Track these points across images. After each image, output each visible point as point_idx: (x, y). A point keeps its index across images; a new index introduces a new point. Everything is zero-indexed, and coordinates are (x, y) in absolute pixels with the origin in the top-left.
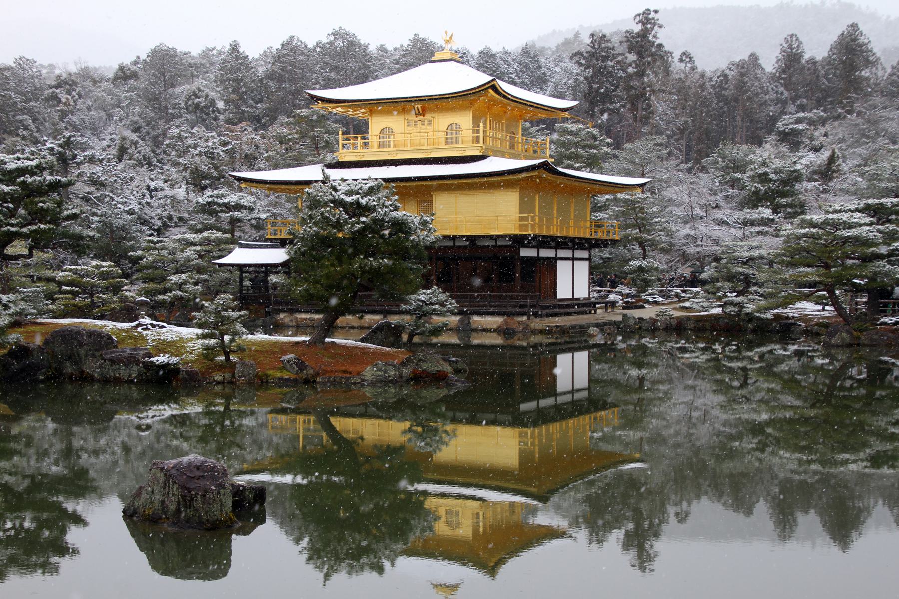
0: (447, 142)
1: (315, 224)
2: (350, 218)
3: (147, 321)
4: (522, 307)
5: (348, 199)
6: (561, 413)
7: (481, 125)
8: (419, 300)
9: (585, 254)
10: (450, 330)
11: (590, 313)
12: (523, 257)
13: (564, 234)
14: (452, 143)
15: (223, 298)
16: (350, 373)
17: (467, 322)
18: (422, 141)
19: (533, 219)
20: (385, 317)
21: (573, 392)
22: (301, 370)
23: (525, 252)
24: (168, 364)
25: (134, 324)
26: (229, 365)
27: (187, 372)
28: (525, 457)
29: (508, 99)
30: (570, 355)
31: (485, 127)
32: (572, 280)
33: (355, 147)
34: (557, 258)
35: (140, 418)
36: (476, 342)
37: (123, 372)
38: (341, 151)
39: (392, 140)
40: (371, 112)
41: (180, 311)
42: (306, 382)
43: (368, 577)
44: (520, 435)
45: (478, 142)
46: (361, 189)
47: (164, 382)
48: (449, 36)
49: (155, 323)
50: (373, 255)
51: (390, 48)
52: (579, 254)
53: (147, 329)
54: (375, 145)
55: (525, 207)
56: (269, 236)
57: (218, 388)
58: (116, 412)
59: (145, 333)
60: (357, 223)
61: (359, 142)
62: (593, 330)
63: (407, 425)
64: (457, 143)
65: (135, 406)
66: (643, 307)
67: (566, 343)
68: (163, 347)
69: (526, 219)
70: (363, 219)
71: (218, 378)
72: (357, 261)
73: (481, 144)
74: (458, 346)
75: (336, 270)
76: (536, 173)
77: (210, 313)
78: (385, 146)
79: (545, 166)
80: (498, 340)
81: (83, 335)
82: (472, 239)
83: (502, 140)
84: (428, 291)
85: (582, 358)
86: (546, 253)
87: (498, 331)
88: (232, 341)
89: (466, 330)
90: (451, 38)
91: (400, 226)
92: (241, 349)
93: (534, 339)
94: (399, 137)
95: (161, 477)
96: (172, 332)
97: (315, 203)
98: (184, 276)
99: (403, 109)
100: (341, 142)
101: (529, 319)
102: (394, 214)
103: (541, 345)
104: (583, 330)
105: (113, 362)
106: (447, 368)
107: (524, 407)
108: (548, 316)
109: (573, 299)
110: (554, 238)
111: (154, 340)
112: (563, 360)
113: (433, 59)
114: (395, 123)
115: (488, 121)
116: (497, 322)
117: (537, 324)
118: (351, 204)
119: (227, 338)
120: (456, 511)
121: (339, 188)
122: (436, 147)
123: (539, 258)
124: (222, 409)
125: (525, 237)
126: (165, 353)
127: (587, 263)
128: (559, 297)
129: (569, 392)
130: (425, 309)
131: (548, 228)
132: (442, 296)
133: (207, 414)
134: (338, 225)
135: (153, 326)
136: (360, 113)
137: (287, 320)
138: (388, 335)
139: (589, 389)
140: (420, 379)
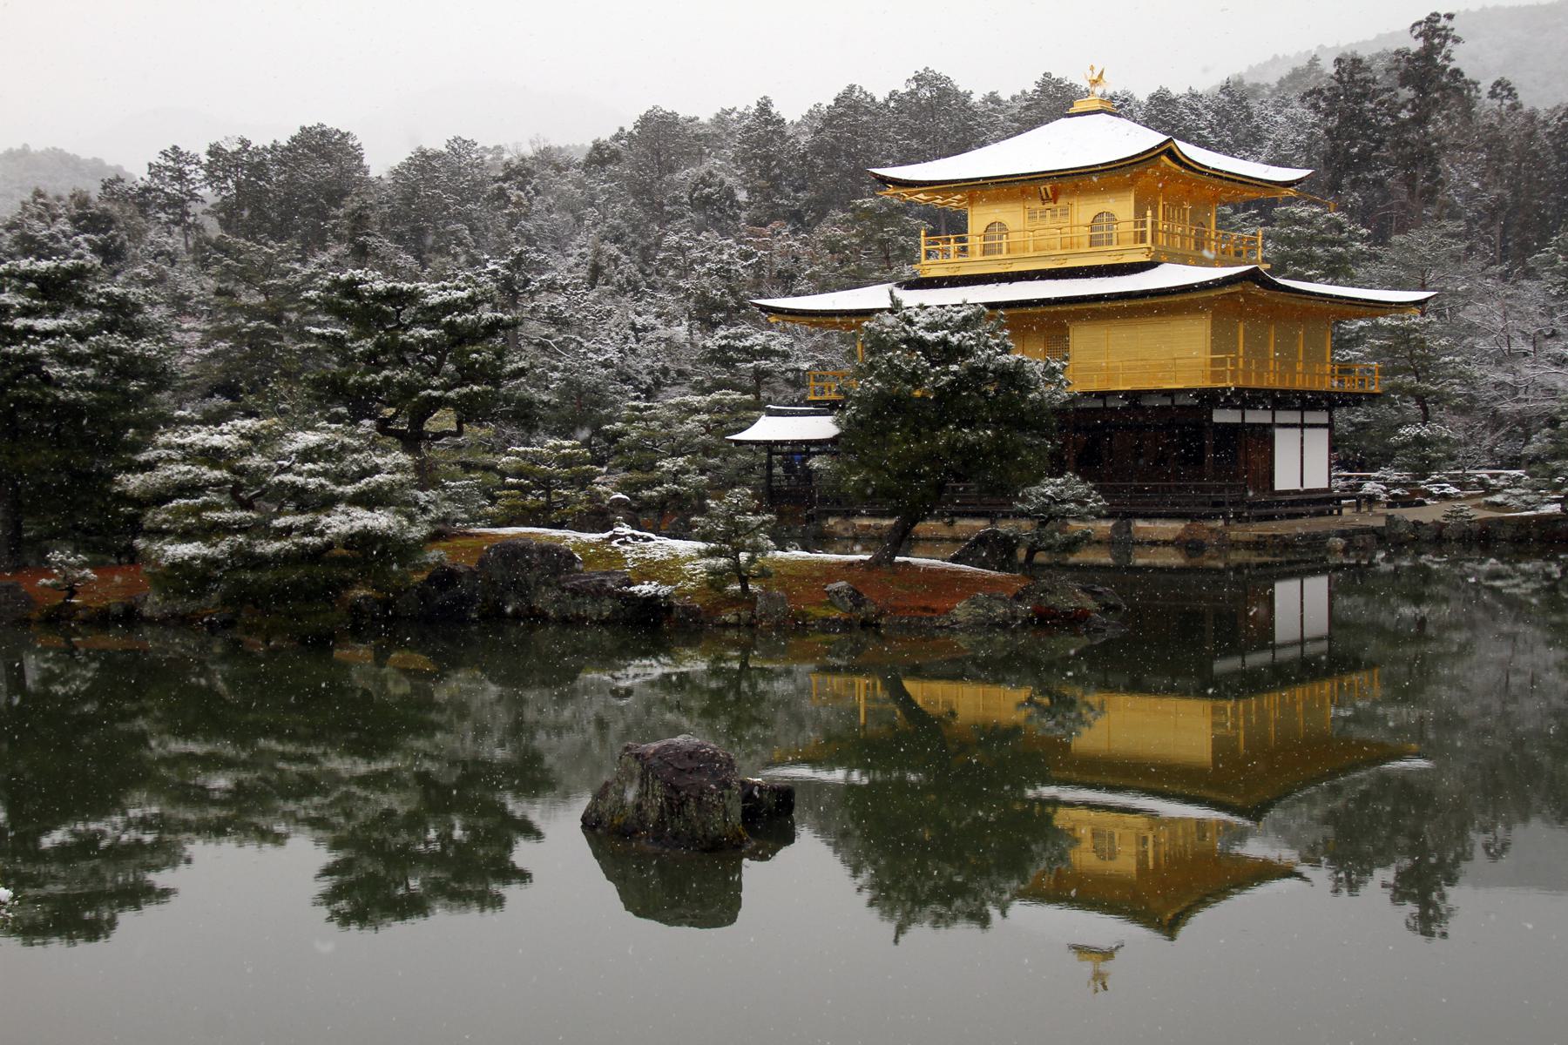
0: (1093, 242)
1: (879, 377)
2: (933, 366)
3: (626, 530)
4: (1216, 504)
5: (930, 337)
6: (1281, 676)
7: (1149, 213)
8: (1043, 495)
9: (1322, 417)
10: (1098, 542)
11: (1331, 513)
12: (1218, 424)
13: (1287, 385)
14: (1100, 244)
15: (738, 495)
16: (934, 611)
18: (1051, 242)
19: (1234, 362)
21: (1302, 642)
22: (858, 606)
23: (1221, 416)
24: (656, 597)
25: (606, 535)
26: (746, 599)
27: (685, 608)
28: (1221, 746)
29: (1194, 170)
30: (1298, 582)
31: (1155, 215)
32: (1301, 461)
33: (946, 253)
35: (617, 679)
36: (1140, 562)
37: (589, 609)
38: (923, 261)
39: (1004, 241)
40: (972, 200)
41: (671, 514)
42: (865, 624)
43: (964, 931)
44: (1215, 711)
45: (1143, 241)
46: (950, 320)
47: (649, 624)
48: (1097, 73)
49: (637, 533)
50: (970, 424)
51: (1005, 96)
53: (625, 543)
54: (978, 250)
55: (1220, 342)
56: (811, 397)
57: (732, 634)
58: (579, 669)
59: (623, 548)
60: (944, 374)
61: (953, 246)
62: (1339, 542)
63: (1023, 694)
64: (1110, 243)
65: (610, 658)
66: (1422, 504)
67: (1290, 563)
68: (649, 570)
69: (1223, 362)
70: (954, 368)
71: (730, 617)
72: (946, 432)
73: (1149, 243)
75: (909, 450)
76: (1238, 288)
77: (718, 517)
78: (993, 253)
79: (1253, 276)
80: (1174, 559)
81: (531, 552)
82: (1134, 396)
83: (1183, 236)
84: (1059, 481)
85: (1318, 587)
87: (1177, 543)
88: (752, 560)
89: (1122, 543)
90: (1101, 75)
91: (1013, 378)
92: (764, 574)
93: (1237, 557)
94: (1015, 237)
95: (636, 767)
96: (662, 547)
97: (879, 344)
98: (680, 461)
99: (1023, 192)
100: (923, 247)
102: (1003, 359)
103: (1248, 566)
104: (1316, 542)
105: (575, 592)
106: (1091, 604)
107: (1221, 666)
108: (1260, 518)
111: (635, 560)
112: (1285, 592)
113: (1072, 111)
114: (1011, 216)
116: (1174, 530)
117: (1238, 532)
118: (936, 344)
119: (743, 556)
120: (1106, 828)
121: (916, 319)
122: (1075, 250)
124: (737, 666)
126: (651, 580)
127: (1326, 431)
128: (1277, 488)
129: (1292, 644)
130: (1053, 508)
131: (1260, 376)
132: (1081, 489)
133: (715, 673)
134: (914, 378)
135: (635, 538)
136: (954, 201)
137: (839, 528)
138: (999, 550)
139: (1330, 638)
140: (1046, 620)
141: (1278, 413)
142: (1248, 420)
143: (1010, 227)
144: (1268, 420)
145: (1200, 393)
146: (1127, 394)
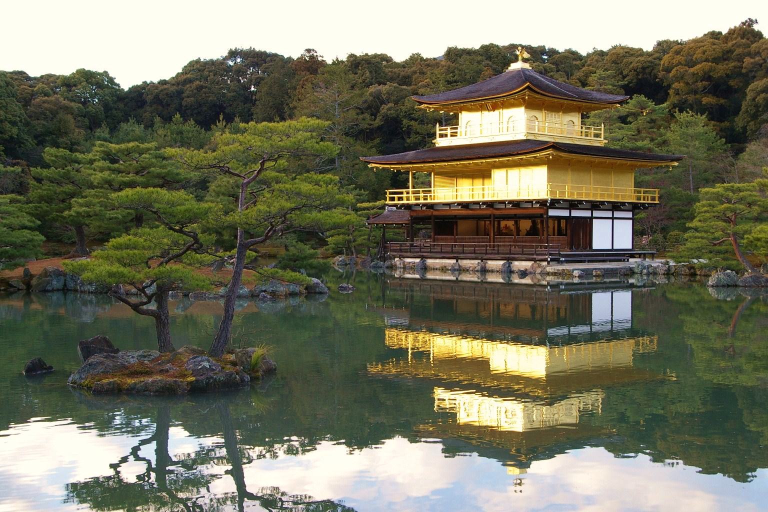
6: (593, 337)
9: (630, 215)
10: (498, 271)
17: (507, 266)
20: (457, 261)
23: (552, 213)
29: (548, 96)
30: (609, 294)
32: (612, 234)
34: (591, 218)
40: (462, 109)
52: (617, 214)
61: (449, 132)
74: (418, 279)
82: (516, 204)
86: (576, 213)
89: (508, 272)
100: (438, 132)
101: (548, 263)
103: (562, 284)
107: (552, 332)
108: (567, 262)
109: (613, 250)
110: (581, 202)
122: (501, 133)
125: (546, 201)
127: (631, 221)
128: (595, 246)
137: (398, 263)
142: (572, 215)
144: (590, 215)
145: (538, 201)
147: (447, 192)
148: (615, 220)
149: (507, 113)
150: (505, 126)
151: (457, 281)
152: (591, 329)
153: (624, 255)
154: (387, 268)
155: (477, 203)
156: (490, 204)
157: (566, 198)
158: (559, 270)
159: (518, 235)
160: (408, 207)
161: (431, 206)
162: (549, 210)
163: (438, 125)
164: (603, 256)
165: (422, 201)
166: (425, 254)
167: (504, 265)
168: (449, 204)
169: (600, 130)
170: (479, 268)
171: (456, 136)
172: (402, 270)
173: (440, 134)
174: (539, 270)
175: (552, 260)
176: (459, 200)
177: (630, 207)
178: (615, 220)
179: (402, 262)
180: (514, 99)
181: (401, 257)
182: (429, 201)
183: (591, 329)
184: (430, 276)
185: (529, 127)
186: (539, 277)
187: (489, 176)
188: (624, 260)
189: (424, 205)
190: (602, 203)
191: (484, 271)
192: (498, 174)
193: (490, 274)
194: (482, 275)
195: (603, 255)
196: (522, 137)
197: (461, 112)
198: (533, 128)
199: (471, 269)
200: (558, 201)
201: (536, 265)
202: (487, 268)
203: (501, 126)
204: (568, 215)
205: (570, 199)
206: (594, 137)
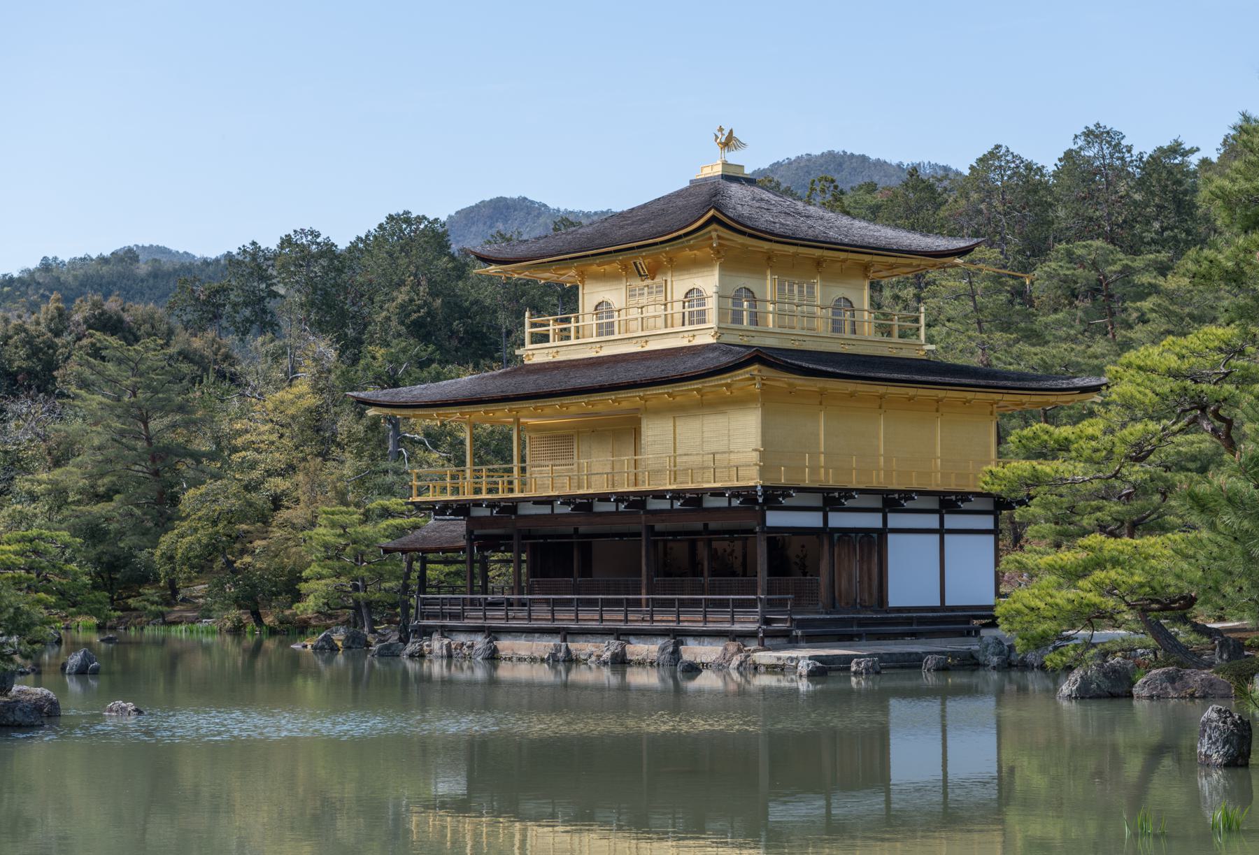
6: (893, 822)
9: (987, 522)
10: (651, 663)
17: (671, 649)
20: (565, 640)
23: (775, 519)
34: (883, 532)
38: (528, 346)
40: (583, 276)
48: (726, 133)
52: (952, 521)
61: (553, 328)
82: (693, 500)
86: (838, 520)
107: (778, 813)
108: (812, 639)
109: (943, 607)
110: (848, 493)
115: (769, 282)
123: (825, 532)
127: (991, 538)
136: (568, 276)
141: (890, 516)
143: (616, 306)
144: (879, 525)
145: (736, 492)
146: (677, 495)
147: (560, 474)
148: (947, 537)
149: (680, 285)
150: (678, 307)
151: (566, 685)
152: (828, 807)
153: (967, 620)
154: (411, 656)
155: (604, 498)
156: (637, 501)
157: (807, 483)
158: (779, 659)
159: (745, 575)
160: (462, 509)
161: (510, 508)
162: (768, 513)
163: (527, 314)
164: (911, 624)
165: (484, 496)
166: (494, 623)
167: (663, 649)
168: (549, 501)
169: (917, 320)
170: (607, 655)
171: (568, 338)
172: (445, 663)
173: (532, 334)
174: (736, 661)
175: (768, 635)
176: (567, 491)
177: (988, 505)
178: (947, 537)
179: (446, 641)
180: (691, 248)
181: (446, 631)
182: (500, 495)
183: (828, 807)
184: (505, 672)
185: (730, 315)
186: (735, 675)
187: (637, 433)
188: (969, 634)
189: (492, 504)
190: (908, 494)
191: (620, 662)
192: (655, 432)
193: (635, 669)
194: (614, 671)
195: (909, 621)
196: (707, 339)
197: (583, 282)
198: (737, 318)
199: (593, 658)
200: (785, 491)
201: (733, 647)
202: (629, 657)
203: (669, 311)
204: (821, 524)
205: (816, 485)
206: (900, 337)
